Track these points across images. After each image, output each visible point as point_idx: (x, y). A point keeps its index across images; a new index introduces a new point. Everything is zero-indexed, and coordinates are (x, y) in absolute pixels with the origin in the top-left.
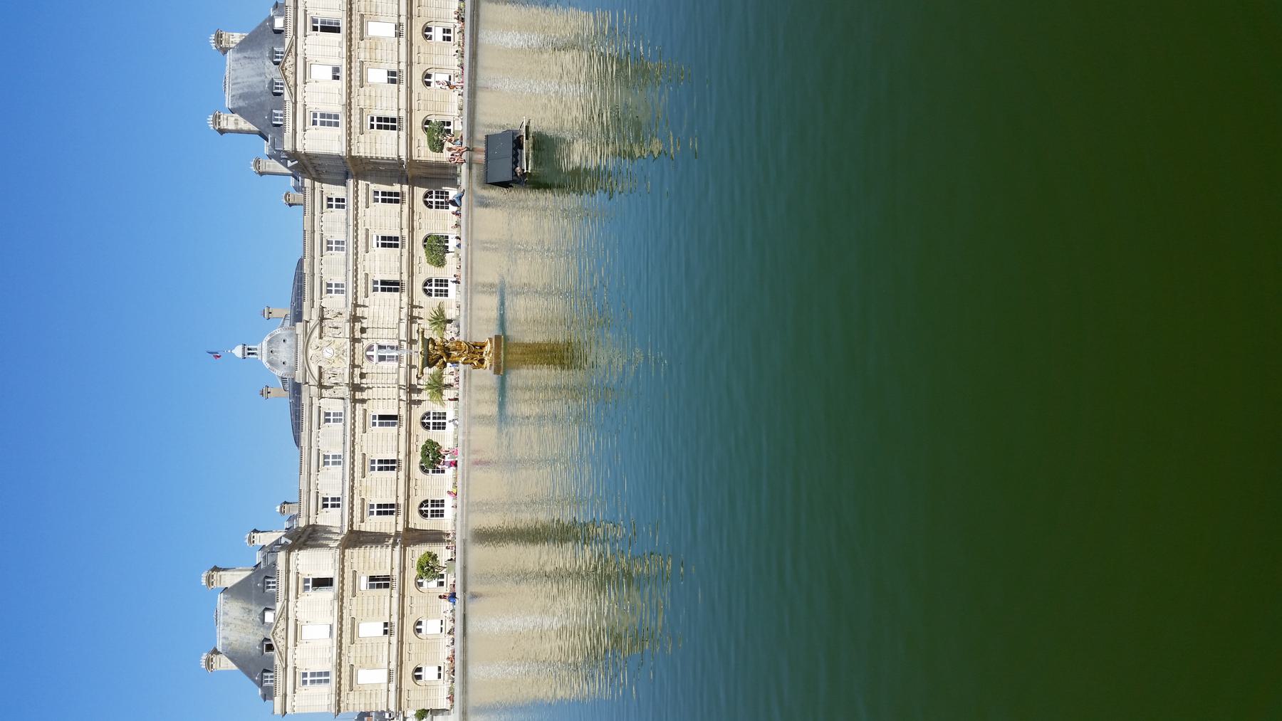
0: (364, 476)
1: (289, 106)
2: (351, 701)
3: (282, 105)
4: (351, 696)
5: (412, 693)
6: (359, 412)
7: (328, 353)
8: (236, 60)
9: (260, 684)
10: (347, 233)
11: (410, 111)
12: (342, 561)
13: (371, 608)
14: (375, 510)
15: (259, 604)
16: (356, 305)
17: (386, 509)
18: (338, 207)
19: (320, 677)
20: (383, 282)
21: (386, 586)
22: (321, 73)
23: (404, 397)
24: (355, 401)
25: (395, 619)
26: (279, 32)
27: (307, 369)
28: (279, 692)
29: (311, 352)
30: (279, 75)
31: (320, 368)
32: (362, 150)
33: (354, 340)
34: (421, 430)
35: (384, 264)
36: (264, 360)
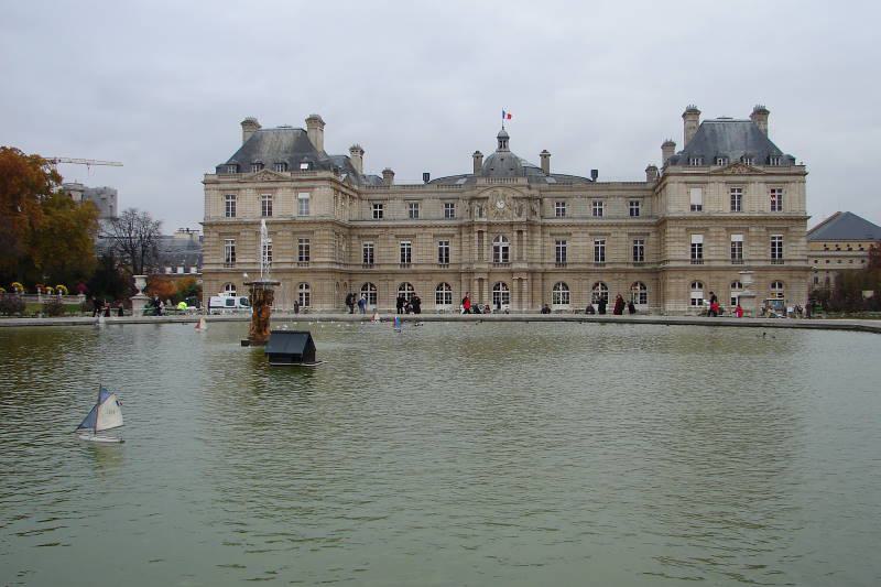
0: (397, 236)
4: (216, 235)
5: (214, 283)
7: (500, 205)
8: (744, 127)
9: (228, 164)
10: (610, 218)
12: (322, 223)
15: (291, 159)
16: (543, 226)
18: (632, 210)
20: (564, 249)
21: (301, 259)
23: (463, 267)
24: (461, 226)
26: (768, 162)
30: (732, 161)
31: (488, 198)
32: (672, 230)
33: (512, 225)
34: (435, 283)
35: (580, 249)
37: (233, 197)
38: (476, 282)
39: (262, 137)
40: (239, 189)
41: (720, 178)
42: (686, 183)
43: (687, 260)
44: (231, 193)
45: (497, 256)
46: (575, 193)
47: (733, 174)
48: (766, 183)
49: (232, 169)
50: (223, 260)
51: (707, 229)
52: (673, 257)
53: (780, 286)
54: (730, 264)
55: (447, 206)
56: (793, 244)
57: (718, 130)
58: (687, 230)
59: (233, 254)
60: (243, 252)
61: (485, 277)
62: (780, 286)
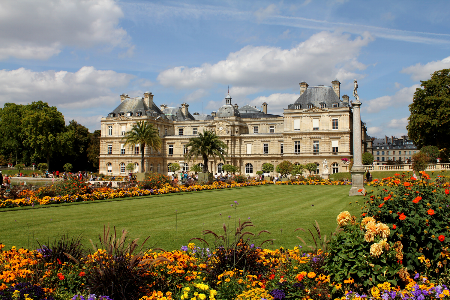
0: (182, 143)
1: (301, 111)
4: (104, 142)
5: (104, 162)
7: (220, 129)
11: (302, 158)
14: (171, 147)
15: (135, 111)
19: (111, 132)
22: (316, 123)
25: (125, 156)
29: (221, 123)
31: (215, 126)
32: (286, 139)
33: (225, 137)
36: (224, 106)
37: (111, 127)
38: (210, 163)
39: (126, 102)
40: (113, 124)
41: (308, 115)
42: (292, 117)
43: (292, 153)
44: (110, 126)
46: (262, 123)
47: (314, 113)
48: (330, 116)
49: (112, 116)
50: (107, 153)
51: (302, 139)
52: (286, 152)
53: (337, 165)
56: (343, 145)
57: (313, 92)
58: (292, 139)
59: (111, 151)
60: (114, 150)
61: (213, 161)
62: (337, 165)
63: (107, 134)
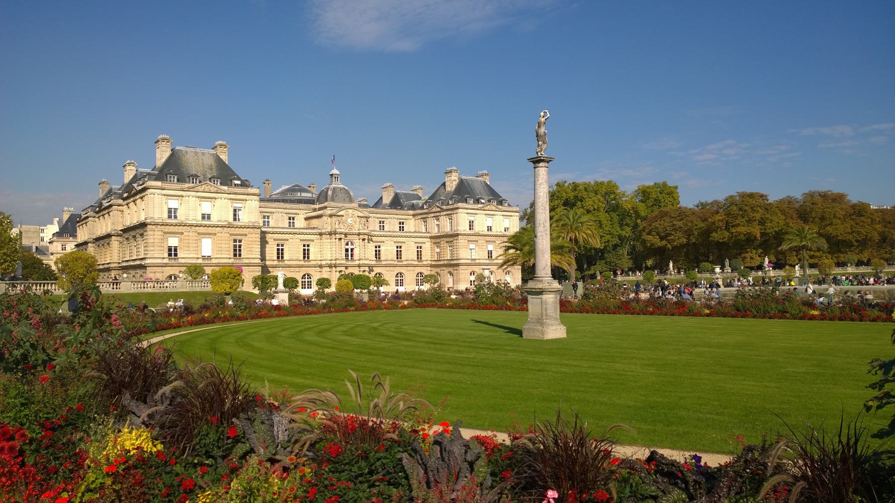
2: (156, 233)
3: (474, 203)
4: (160, 233)
6: (312, 237)
7: (349, 220)
11: (480, 264)
13: (223, 246)
17: (280, 254)
21: (235, 255)
23: (324, 263)
24: (321, 234)
25: (214, 261)
27: (341, 209)
28: (165, 185)
33: (359, 234)
35: (388, 250)
45: (347, 255)
50: (166, 255)
54: (488, 261)
55: (290, 219)
63: (166, 215)
